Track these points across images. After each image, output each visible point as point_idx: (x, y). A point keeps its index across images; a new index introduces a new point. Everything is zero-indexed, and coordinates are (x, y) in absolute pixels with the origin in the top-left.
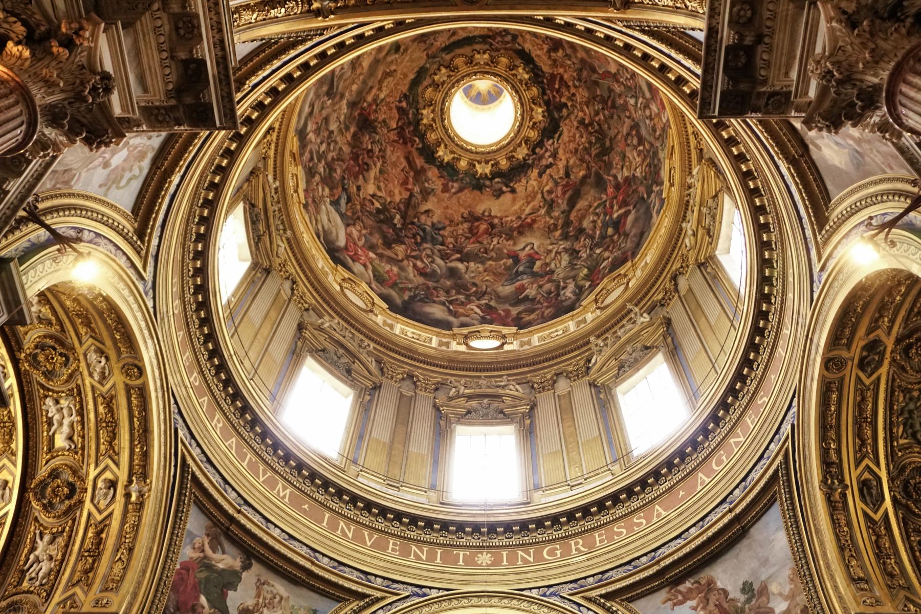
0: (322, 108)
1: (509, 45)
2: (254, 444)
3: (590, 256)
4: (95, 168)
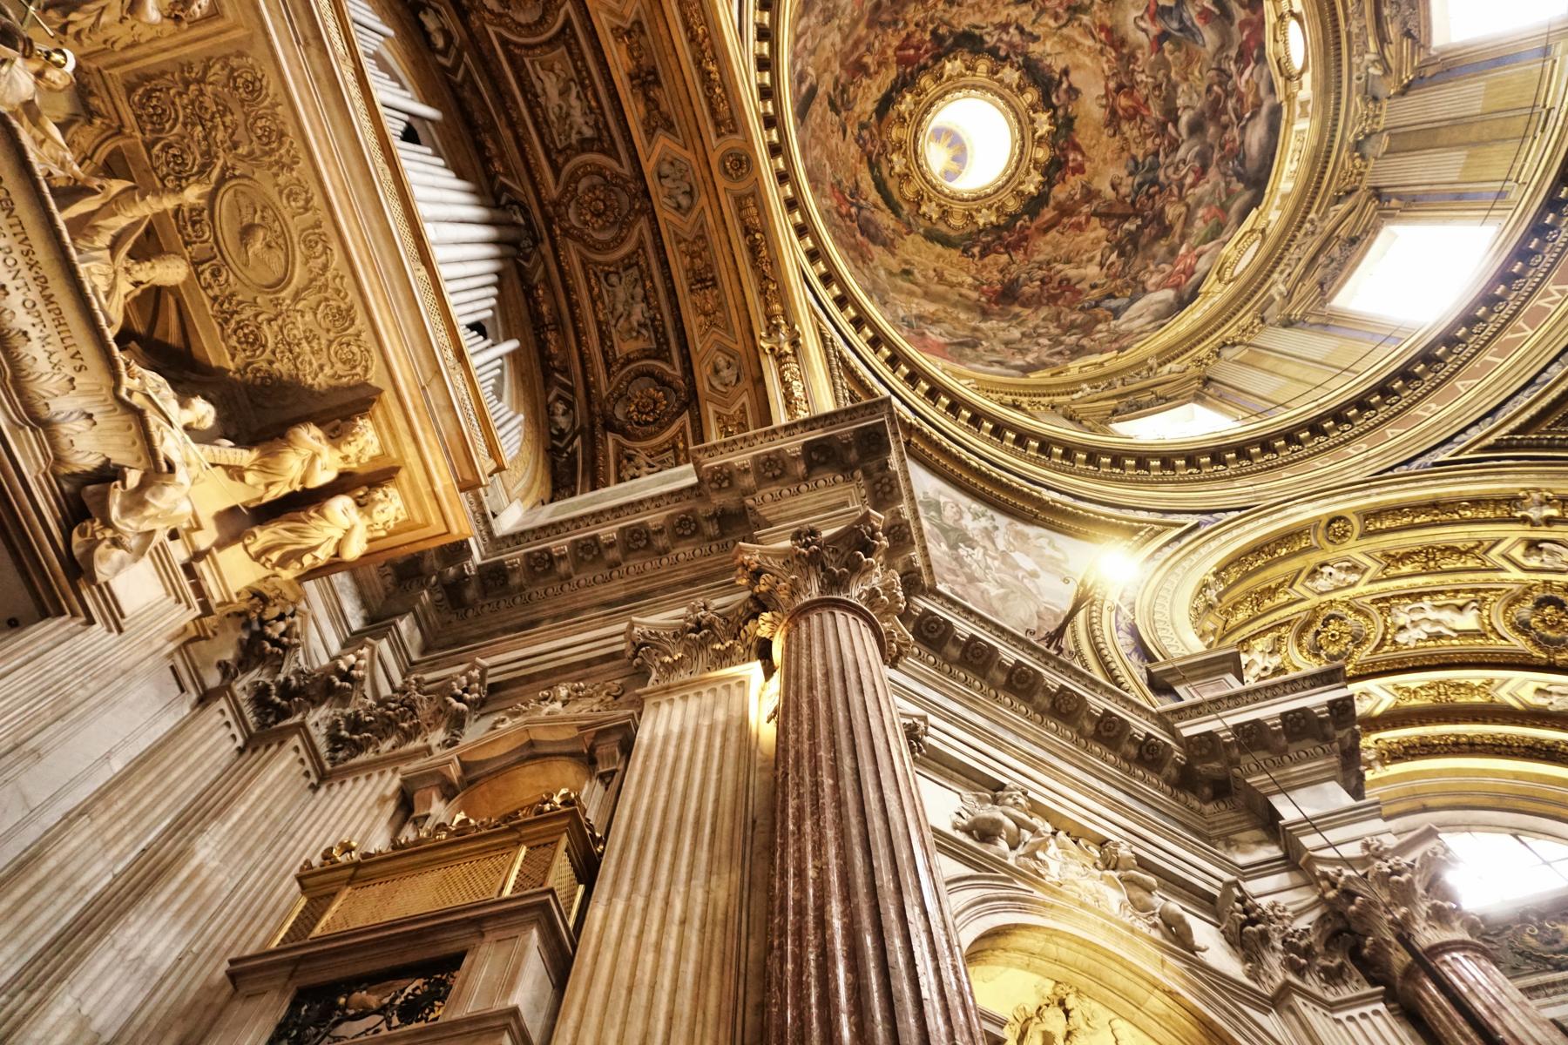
0: (993, 350)
2: (1467, 353)
4: (1038, 588)
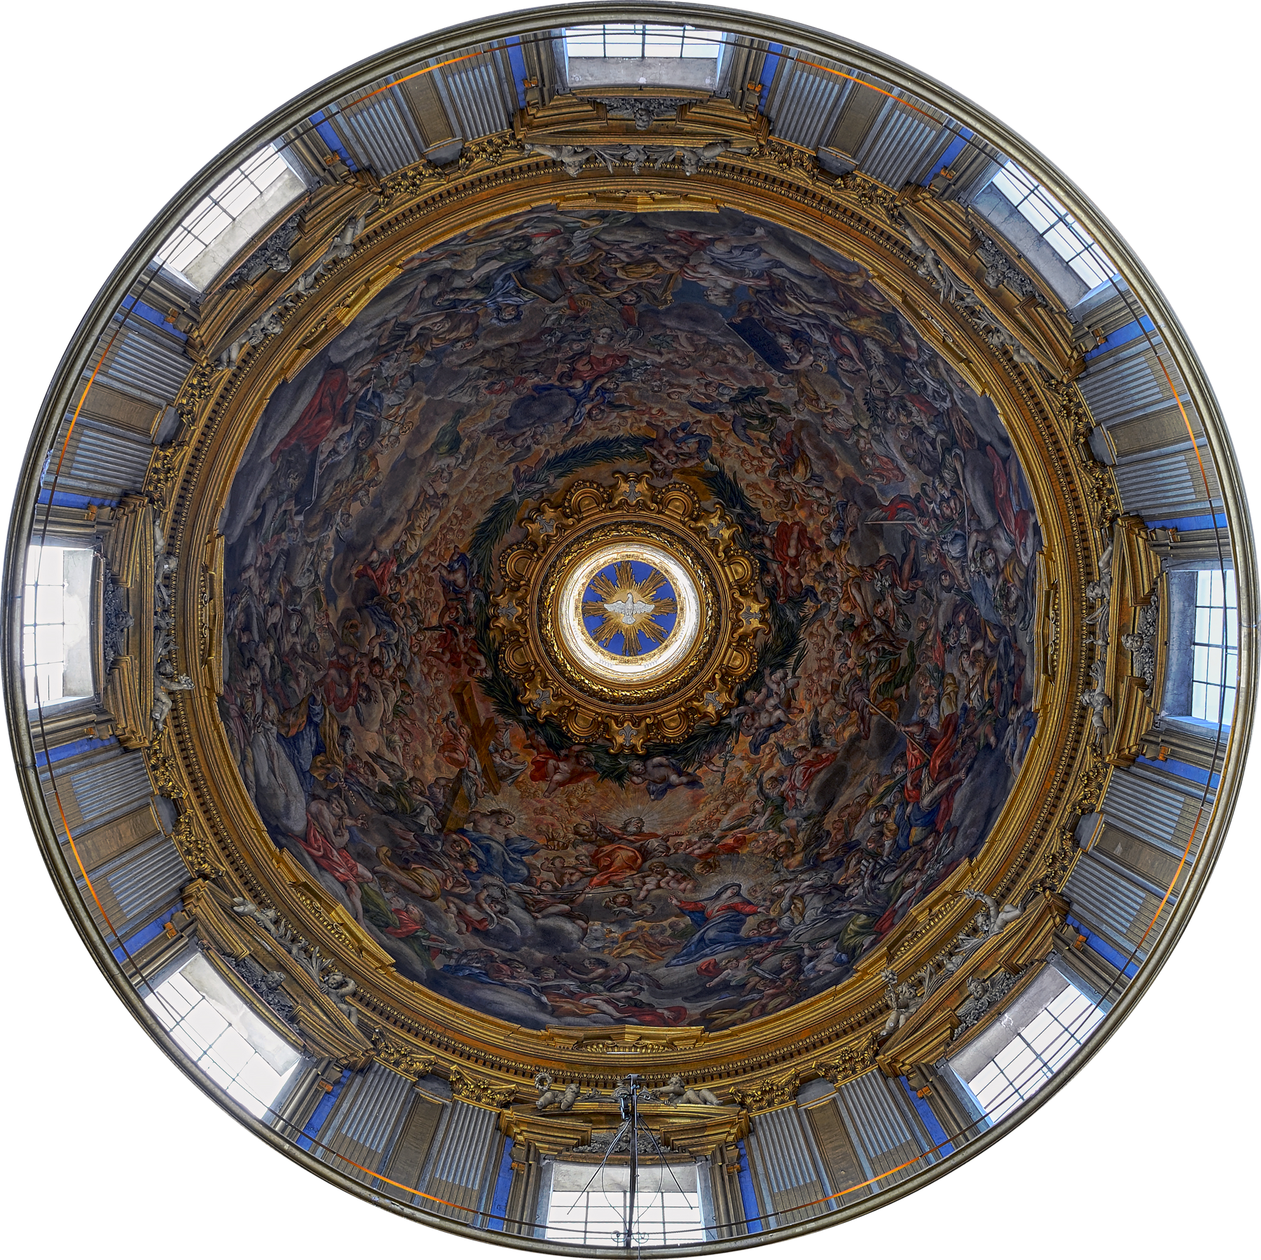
0: (283, 527)
1: (691, 463)
3: (872, 890)
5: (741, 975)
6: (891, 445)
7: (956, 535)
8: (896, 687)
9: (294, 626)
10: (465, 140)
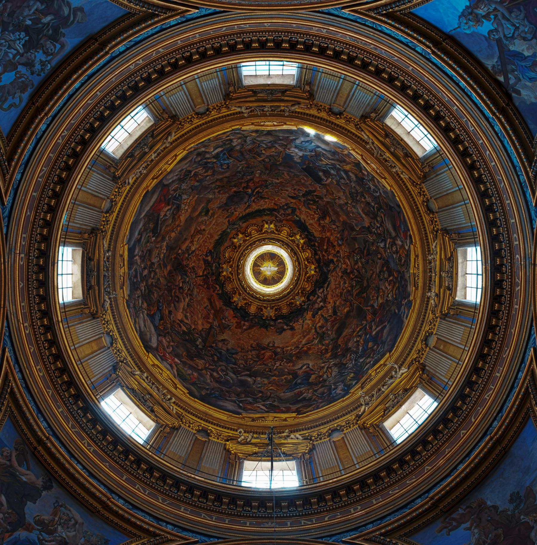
0: (148, 242)
3: (355, 364)
5: (310, 395)
6: (359, 209)
7: (383, 240)
8: (363, 294)
9: (152, 276)
10: (208, 105)
